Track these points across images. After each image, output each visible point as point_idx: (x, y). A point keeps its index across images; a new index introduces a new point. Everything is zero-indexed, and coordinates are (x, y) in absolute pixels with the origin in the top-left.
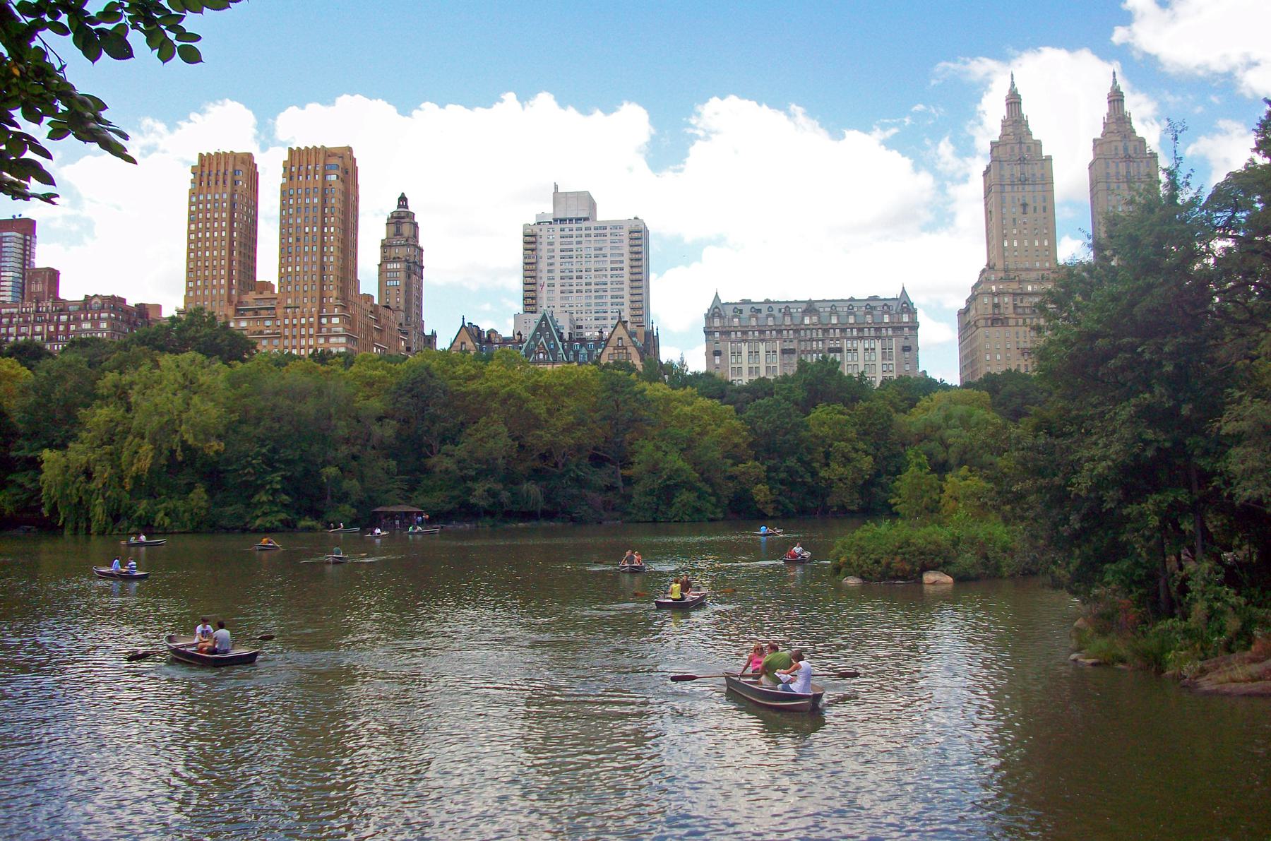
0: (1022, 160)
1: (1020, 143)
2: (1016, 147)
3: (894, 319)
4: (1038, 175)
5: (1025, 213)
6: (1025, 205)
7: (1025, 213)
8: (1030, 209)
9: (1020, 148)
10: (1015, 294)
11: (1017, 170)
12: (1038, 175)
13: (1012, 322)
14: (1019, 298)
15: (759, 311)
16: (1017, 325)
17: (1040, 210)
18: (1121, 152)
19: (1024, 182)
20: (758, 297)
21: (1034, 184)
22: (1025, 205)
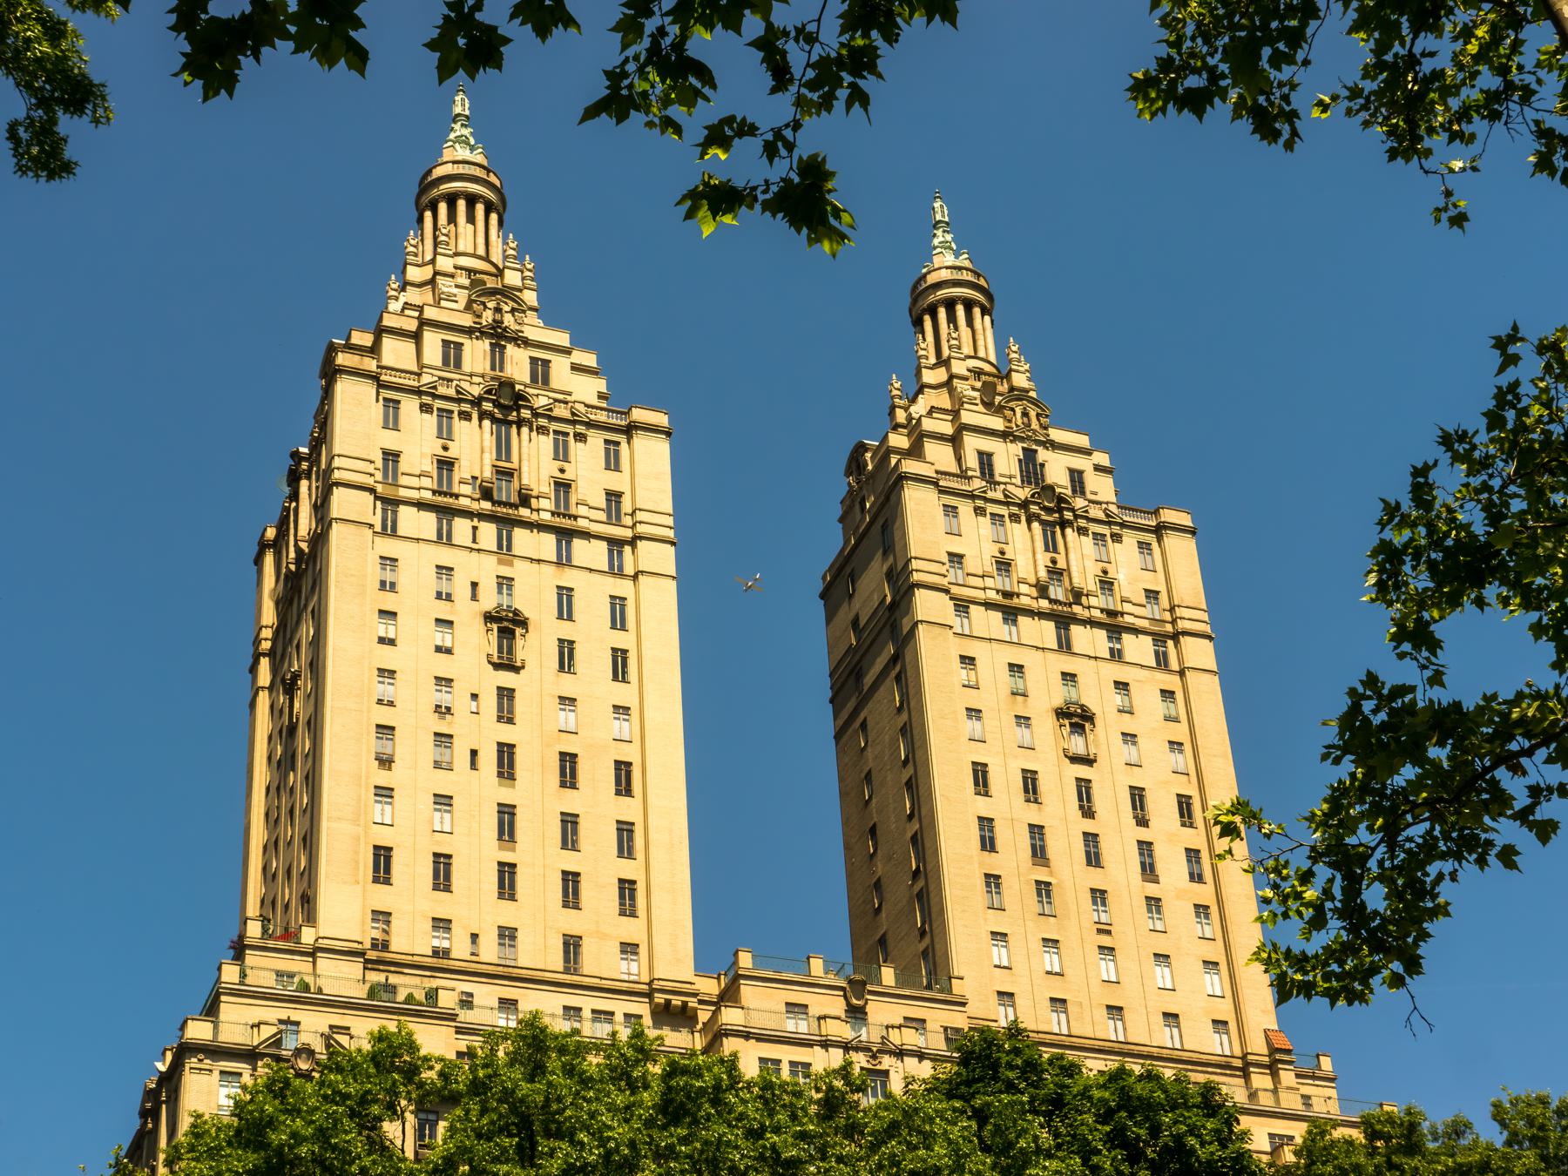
5: (506, 663)
7: (506, 663)
8: (536, 648)
19: (504, 506)
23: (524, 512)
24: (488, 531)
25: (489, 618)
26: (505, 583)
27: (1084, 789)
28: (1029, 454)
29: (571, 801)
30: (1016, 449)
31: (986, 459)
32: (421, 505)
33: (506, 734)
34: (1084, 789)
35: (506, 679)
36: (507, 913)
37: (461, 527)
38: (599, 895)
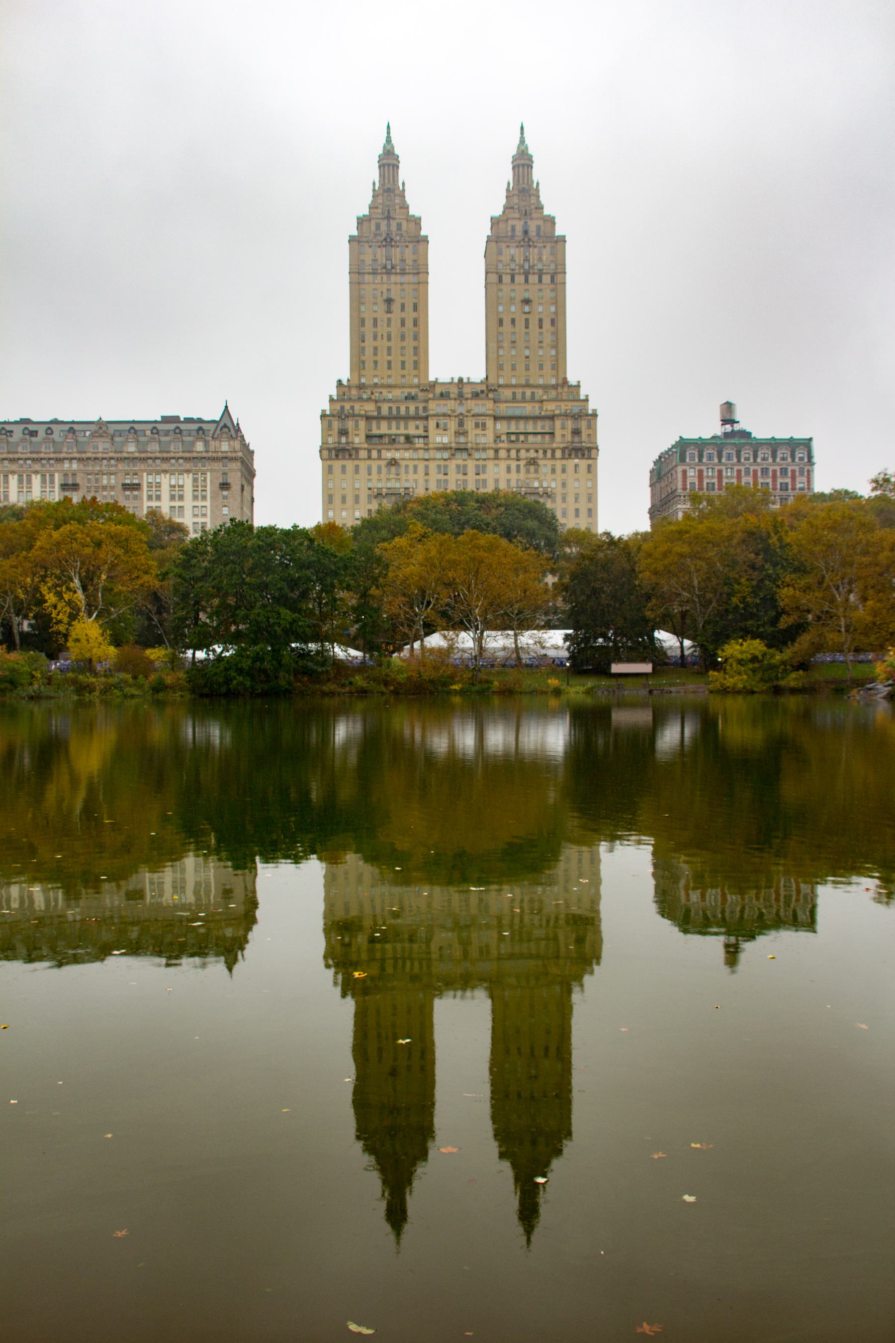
0: (388, 242)
1: (388, 218)
2: (383, 224)
3: (218, 447)
4: (409, 262)
5: (389, 311)
6: (389, 301)
7: (389, 311)
8: (396, 307)
9: (389, 226)
10: (368, 418)
11: (381, 254)
12: (409, 262)
13: (363, 454)
14: (374, 423)
15: (34, 434)
16: (369, 458)
17: (409, 307)
18: (519, 232)
19: (389, 271)
20: (40, 414)
21: (403, 273)
22: (389, 301)
23: (393, 271)
24: (385, 277)
25: (385, 301)
26: (388, 290)
27: (527, 320)
28: (526, 223)
29: (404, 344)
30: (522, 222)
31: (513, 228)
32: (369, 273)
33: (389, 329)
34: (527, 320)
35: (389, 315)
36: (389, 373)
37: (379, 277)
38: (409, 365)
